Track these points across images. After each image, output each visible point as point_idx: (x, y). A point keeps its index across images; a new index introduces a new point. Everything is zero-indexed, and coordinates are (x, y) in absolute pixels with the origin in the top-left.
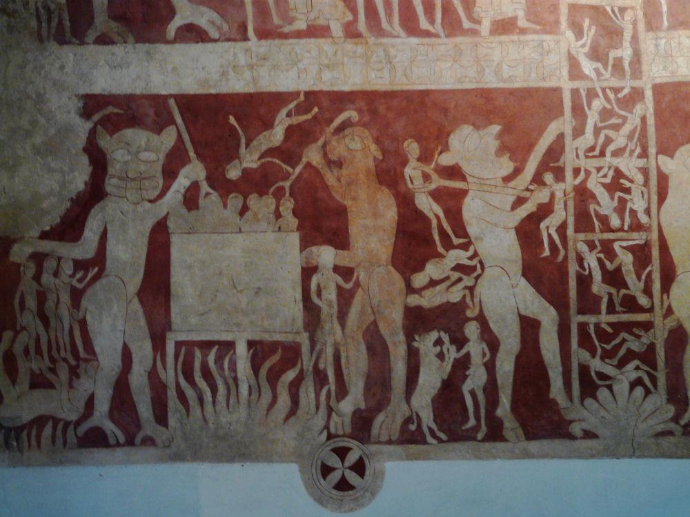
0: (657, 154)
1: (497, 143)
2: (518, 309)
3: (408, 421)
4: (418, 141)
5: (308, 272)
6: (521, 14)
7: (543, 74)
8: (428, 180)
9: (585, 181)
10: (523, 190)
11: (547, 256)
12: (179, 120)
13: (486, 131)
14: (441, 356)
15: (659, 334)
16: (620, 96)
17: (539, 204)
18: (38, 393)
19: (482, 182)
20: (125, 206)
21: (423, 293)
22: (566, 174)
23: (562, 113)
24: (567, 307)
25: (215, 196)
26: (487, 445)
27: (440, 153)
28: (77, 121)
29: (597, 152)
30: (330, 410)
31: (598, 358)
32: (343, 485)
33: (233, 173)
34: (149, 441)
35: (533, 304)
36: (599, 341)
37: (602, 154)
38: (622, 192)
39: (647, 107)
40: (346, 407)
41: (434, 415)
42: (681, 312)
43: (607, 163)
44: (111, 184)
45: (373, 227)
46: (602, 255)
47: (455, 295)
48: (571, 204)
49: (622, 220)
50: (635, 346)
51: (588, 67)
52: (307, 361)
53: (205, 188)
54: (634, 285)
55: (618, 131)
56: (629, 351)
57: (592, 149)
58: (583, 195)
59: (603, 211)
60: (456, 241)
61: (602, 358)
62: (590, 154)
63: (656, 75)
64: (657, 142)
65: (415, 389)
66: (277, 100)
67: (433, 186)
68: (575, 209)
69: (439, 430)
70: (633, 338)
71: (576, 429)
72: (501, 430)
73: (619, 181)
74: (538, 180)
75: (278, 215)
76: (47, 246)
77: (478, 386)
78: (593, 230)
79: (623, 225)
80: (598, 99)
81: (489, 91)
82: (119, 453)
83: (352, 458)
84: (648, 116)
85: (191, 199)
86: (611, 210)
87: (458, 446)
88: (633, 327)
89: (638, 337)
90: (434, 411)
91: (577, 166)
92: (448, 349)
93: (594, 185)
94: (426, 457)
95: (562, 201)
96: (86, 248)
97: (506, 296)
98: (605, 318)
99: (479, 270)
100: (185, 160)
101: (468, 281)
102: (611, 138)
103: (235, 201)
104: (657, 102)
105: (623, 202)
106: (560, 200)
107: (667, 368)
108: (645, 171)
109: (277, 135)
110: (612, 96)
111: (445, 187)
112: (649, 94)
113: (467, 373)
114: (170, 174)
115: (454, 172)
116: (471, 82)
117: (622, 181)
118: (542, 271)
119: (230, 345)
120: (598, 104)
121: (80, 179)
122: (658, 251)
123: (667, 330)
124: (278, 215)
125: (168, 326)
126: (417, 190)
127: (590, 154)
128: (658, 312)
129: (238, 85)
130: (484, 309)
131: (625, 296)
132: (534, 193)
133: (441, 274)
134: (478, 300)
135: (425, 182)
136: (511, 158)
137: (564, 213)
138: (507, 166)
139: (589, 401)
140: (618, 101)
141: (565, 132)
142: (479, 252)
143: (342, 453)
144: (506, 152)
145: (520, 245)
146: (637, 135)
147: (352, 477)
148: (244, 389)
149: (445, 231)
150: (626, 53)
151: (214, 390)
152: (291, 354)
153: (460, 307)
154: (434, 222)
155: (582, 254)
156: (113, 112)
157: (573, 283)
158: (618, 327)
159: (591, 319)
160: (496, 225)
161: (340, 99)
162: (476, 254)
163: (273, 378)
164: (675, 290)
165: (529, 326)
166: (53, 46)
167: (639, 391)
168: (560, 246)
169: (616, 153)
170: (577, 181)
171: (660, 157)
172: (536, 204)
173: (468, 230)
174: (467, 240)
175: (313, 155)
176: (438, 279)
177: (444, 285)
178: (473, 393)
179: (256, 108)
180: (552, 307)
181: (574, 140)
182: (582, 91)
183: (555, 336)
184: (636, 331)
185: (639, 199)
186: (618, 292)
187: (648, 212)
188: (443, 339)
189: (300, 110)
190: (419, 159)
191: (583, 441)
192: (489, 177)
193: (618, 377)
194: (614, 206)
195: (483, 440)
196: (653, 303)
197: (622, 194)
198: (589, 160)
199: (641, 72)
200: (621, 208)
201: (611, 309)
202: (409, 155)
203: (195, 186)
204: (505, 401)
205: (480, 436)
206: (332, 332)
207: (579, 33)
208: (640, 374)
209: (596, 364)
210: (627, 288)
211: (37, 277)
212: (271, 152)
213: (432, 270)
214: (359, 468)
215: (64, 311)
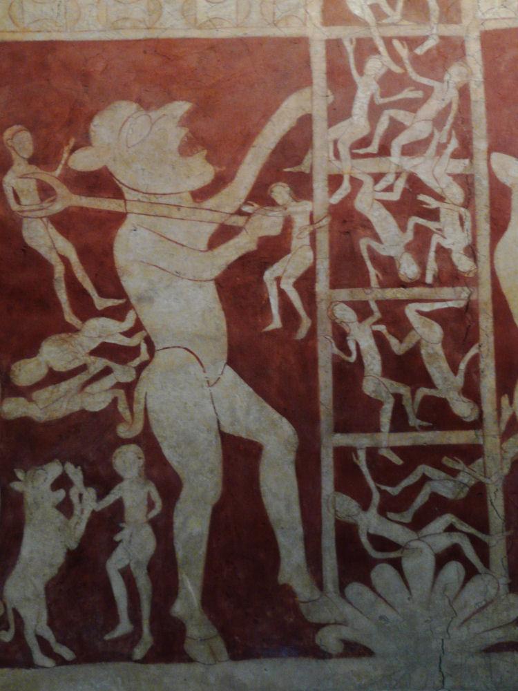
0: (491, 150)
1: (183, 132)
2: (218, 422)
4: (31, 129)
7: (274, 14)
8: (49, 196)
9: (351, 197)
10: (232, 214)
11: (277, 330)
13: (160, 112)
14: (66, 507)
15: (490, 464)
16: (419, 51)
17: (260, 238)
19: (153, 199)
21: (35, 395)
22: (315, 185)
23: (308, 82)
24: (314, 418)
26: (153, 669)
27: (73, 151)
29: (374, 148)
31: (373, 511)
35: (248, 413)
36: (376, 479)
37: (384, 151)
38: (422, 216)
39: (471, 70)
41: (50, 614)
43: (393, 166)
46: (382, 328)
47: (97, 399)
48: (323, 238)
49: (423, 265)
50: (445, 488)
54: (446, 379)
55: (415, 111)
56: (435, 498)
57: (365, 142)
58: (346, 222)
59: (384, 250)
60: (100, 303)
61: (382, 511)
62: (361, 151)
63: (488, 16)
64: (489, 131)
65: (13, 565)
67: (58, 207)
68: (331, 246)
69: (58, 641)
70: (443, 474)
71: (329, 639)
72: (183, 642)
73: (416, 197)
74: (260, 195)
77: (138, 562)
78: (366, 283)
79: (423, 275)
80: (377, 56)
81: (170, 43)
84: (473, 86)
86: (400, 249)
88: (442, 457)
89: (453, 473)
90: (49, 607)
91: (335, 172)
92: (81, 496)
93: (367, 204)
95: (307, 233)
97: (195, 397)
98: (387, 439)
99: (144, 355)
101: (123, 374)
102: (402, 124)
105: (423, 236)
106: (302, 230)
108: (466, 182)
110: (403, 52)
111: (82, 208)
112: (474, 48)
113: (117, 538)
115: (100, 182)
116: (135, 28)
117: (422, 197)
118: (265, 352)
120: (376, 65)
122: (491, 320)
123: (509, 461)
126: (25, 214)
127: (361, 151)
128: (492, 428)
130: (153, 423)
131: (426, 399)
132: (253, 218)
133: (70, 362)
134: (142, 407)
135: (42, 200)
136: (209, 159)
137: (310, 254)
138: (201, 171)
139: (355, 589)
140: (416, 60)
141: (315, 113)
142: (145, 323)
144: (200, 148)
145: (224, 309)
146: (450, 120)
149: (79, 284)
153: (110, 417)
154: (59, 270)
155: (344, 325)
157: (325, 378)
158: (413, 455)
159: (361, 441)
160: (178, 274)
162: (138, 327)
165: (240, 455)
167: (453, 571)
168: (302, 313)
169: (409, 151)
170: (336, 198)
171: (495, 156)
172: (256, 238)
173: (124, 284)
174: (121, 302)
176: (64, 370)
177: (75, 382)
178: (127, 575)
180: (285, 420)
181: (330, 125)
182: (346, 43)
183: (291, 471)
184: (447, 461)
185: (455, 230)
186: (413, 393)
187: (471, 251)
188: (71, 476)
190: (32, 161)
191: (342, 661)
192: (168, 191)
193: (415, 544)
194: (407, 241)
195: (145, 660)
196: (481, 413)
197: (421, 221)
198: (361, 161)
199: (459, 11)
201: (400, 422)
202: (14, 155)
204: (190, 588)
205: (139, 652)
208: (456, 538)
209: (370, 522)
210: (429, 383)
213: (53, 354)
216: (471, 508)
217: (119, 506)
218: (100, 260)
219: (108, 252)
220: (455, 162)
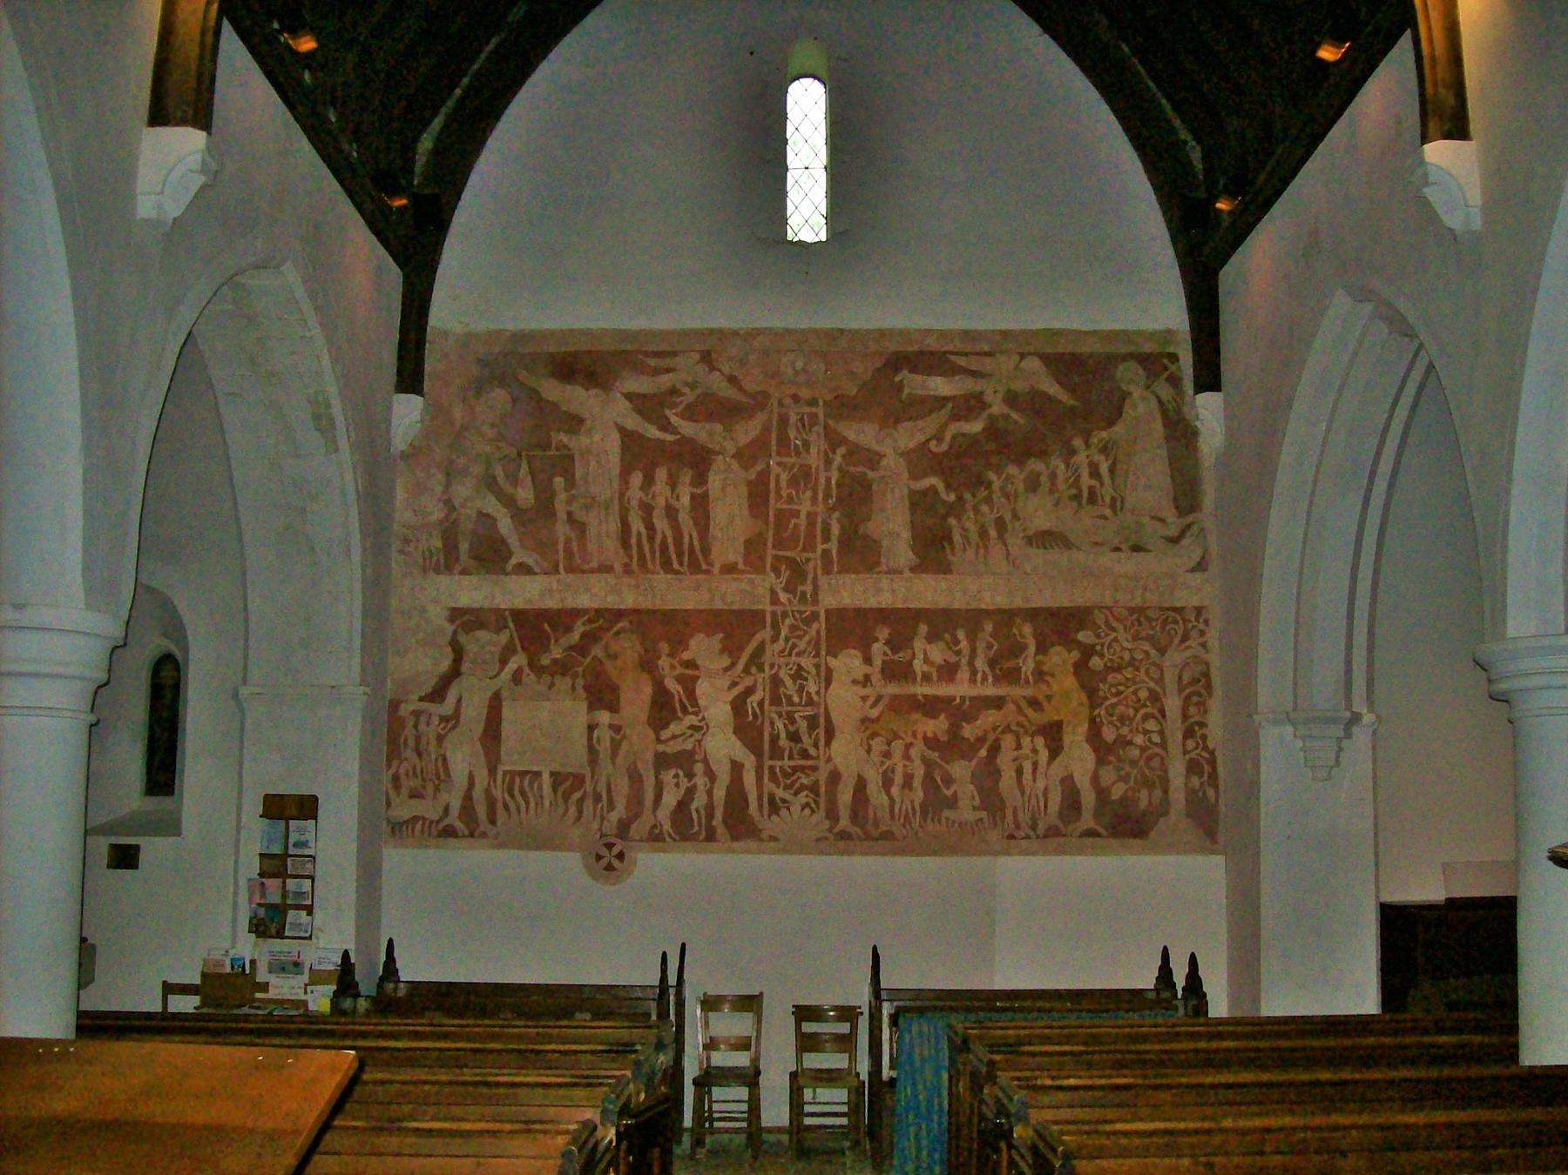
3: (655, 826)
5: (591, 728)
6: (740, 561)
12: (512, 625)
14: (677, 785)
18: (413, 802)
20: (473, 680)
25: (532, 676)
28: (447, 625)
30: (603, 818)
32: (610, 868)
33: (545, 661)
34: (484, 835)
40: (614, 817)
42: (838, 760)
44: (465, 667)
45: (636, 698)
47: (689, 746)
50: (805, 781)
51: (783, 597)
52: (588, 787)
53: (527, 670)
58: (776, 682)
66: (575, 613)
71: (764, 835)
74: (746, 670)
75: (573, 687)
76: (425, 705)
82: (465, 842)
83: (615, 851)
85: (517, 678)
87: (688, 844)
94: (664, 851)
96: (447, 707)
97: (722, 745)
98: (787, 763)
100: (514, 652)
101: (697, 736)
103: (546, 678)
104: (827, 619)
105: (802, 688)
108: (817, 666)
109: (575, 637)
112: (822, 615)
114: (504, 662)
115: (691, 664)
118: (746, 728)
119: (538, 774)
120: (788, 621)
121: (446, 664)
124: (573, 687)
125: (498, 759)
129: (551, 603)
138: (725, 661)
139: (774, 817)
140: (803, 621)
143: (609, 846)
147: (616, 863)
148: (547, 803)
150: (808, 588)
151: (527, 803)
152: (579, 780)
156: (467, 620)
158: (795, 769)
159: (779, 763)
161: (620, 614)
163: (566, 799)
164: (834, 744)
165: (737, 767)
166: (432, 575)
167: (807, 811)
175: (597, 651)
178: (697, 811)
179: (563, 619)
187: (818, 693)
189: (590, 621)
200: (801, 689)
201: (791, 757)
203: (519, 671)
206: (606, 767)
207: (778, 575)
209: (780, 793)
211: (416, 726)
212: (571, 648)
213: (674, 728)
214: (621, 856)
215: (433, 747)
216: (814, 788)
217: (695, 786)
218: (691, 694)
219: (694, 690)
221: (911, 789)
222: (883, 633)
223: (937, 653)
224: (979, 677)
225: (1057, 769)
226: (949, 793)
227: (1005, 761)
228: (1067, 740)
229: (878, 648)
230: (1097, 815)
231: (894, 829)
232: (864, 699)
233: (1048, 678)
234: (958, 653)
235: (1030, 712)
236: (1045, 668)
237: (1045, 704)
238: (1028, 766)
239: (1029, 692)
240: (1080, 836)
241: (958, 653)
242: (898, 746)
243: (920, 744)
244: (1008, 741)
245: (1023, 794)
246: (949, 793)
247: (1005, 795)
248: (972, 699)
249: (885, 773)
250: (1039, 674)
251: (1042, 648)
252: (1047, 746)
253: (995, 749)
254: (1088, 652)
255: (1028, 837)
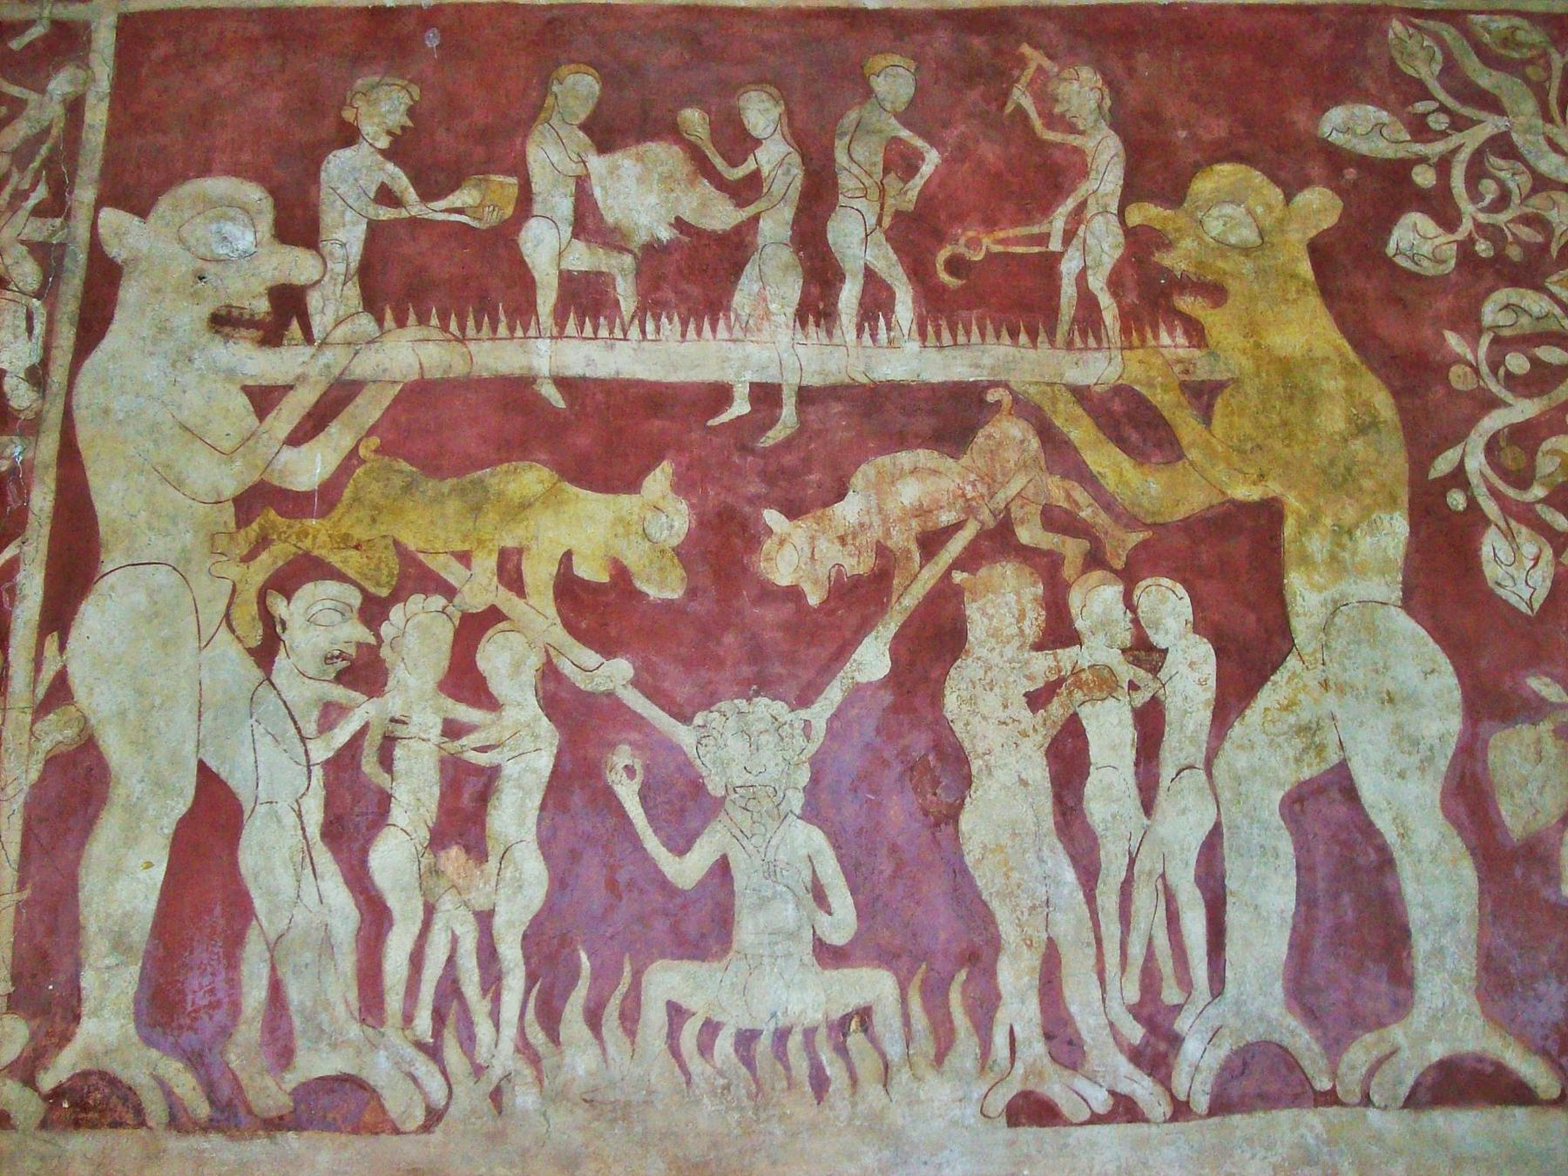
42: (98, 696)
84: (91, 100)
107: (21, 884)
108: (48, 256)
112: (104, 39)
122: (51, 497)
123: (41, 756)
146: (44, 150)
171: (109, 216)
185: (16, 337)
187: (37, 376)
220: (38, 222)
221: (477, 850)
222: (383, 108)
223: (645, 194)
224: (849, 295)
225: (1265, 757)
226: (687, 870)
227: (987, 705)
228: (1306, 596)
229: (352, 181)
230: (1497, 983)
231: (380, 1070)
232: (264, 399)
233: (1187, 303)
234: (748, 190)
235: (1105, 460)
236: (1176, 261)
237: (1187, 427)
238: (1109, 731)
239: (1099, 368)
240: (1413, 1101)
241: (748, 190)
242: (418, 636)
243: (538, 612)
244: (1001, 607)
245: (1089, 875)
246: (687, 870)
247: (987, 880)
248: (806, 396)
249: (343, 764)
250: (1151, 291)
251: (1156, 172)
252: (1203, 624)
253: (936, 639)
254: (1383, 191)
255: (1125, 1110)
